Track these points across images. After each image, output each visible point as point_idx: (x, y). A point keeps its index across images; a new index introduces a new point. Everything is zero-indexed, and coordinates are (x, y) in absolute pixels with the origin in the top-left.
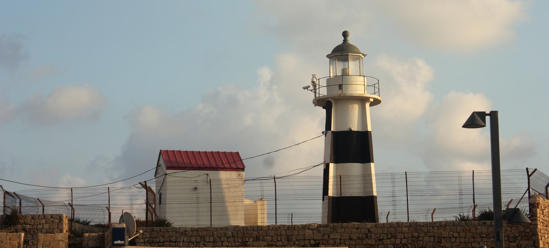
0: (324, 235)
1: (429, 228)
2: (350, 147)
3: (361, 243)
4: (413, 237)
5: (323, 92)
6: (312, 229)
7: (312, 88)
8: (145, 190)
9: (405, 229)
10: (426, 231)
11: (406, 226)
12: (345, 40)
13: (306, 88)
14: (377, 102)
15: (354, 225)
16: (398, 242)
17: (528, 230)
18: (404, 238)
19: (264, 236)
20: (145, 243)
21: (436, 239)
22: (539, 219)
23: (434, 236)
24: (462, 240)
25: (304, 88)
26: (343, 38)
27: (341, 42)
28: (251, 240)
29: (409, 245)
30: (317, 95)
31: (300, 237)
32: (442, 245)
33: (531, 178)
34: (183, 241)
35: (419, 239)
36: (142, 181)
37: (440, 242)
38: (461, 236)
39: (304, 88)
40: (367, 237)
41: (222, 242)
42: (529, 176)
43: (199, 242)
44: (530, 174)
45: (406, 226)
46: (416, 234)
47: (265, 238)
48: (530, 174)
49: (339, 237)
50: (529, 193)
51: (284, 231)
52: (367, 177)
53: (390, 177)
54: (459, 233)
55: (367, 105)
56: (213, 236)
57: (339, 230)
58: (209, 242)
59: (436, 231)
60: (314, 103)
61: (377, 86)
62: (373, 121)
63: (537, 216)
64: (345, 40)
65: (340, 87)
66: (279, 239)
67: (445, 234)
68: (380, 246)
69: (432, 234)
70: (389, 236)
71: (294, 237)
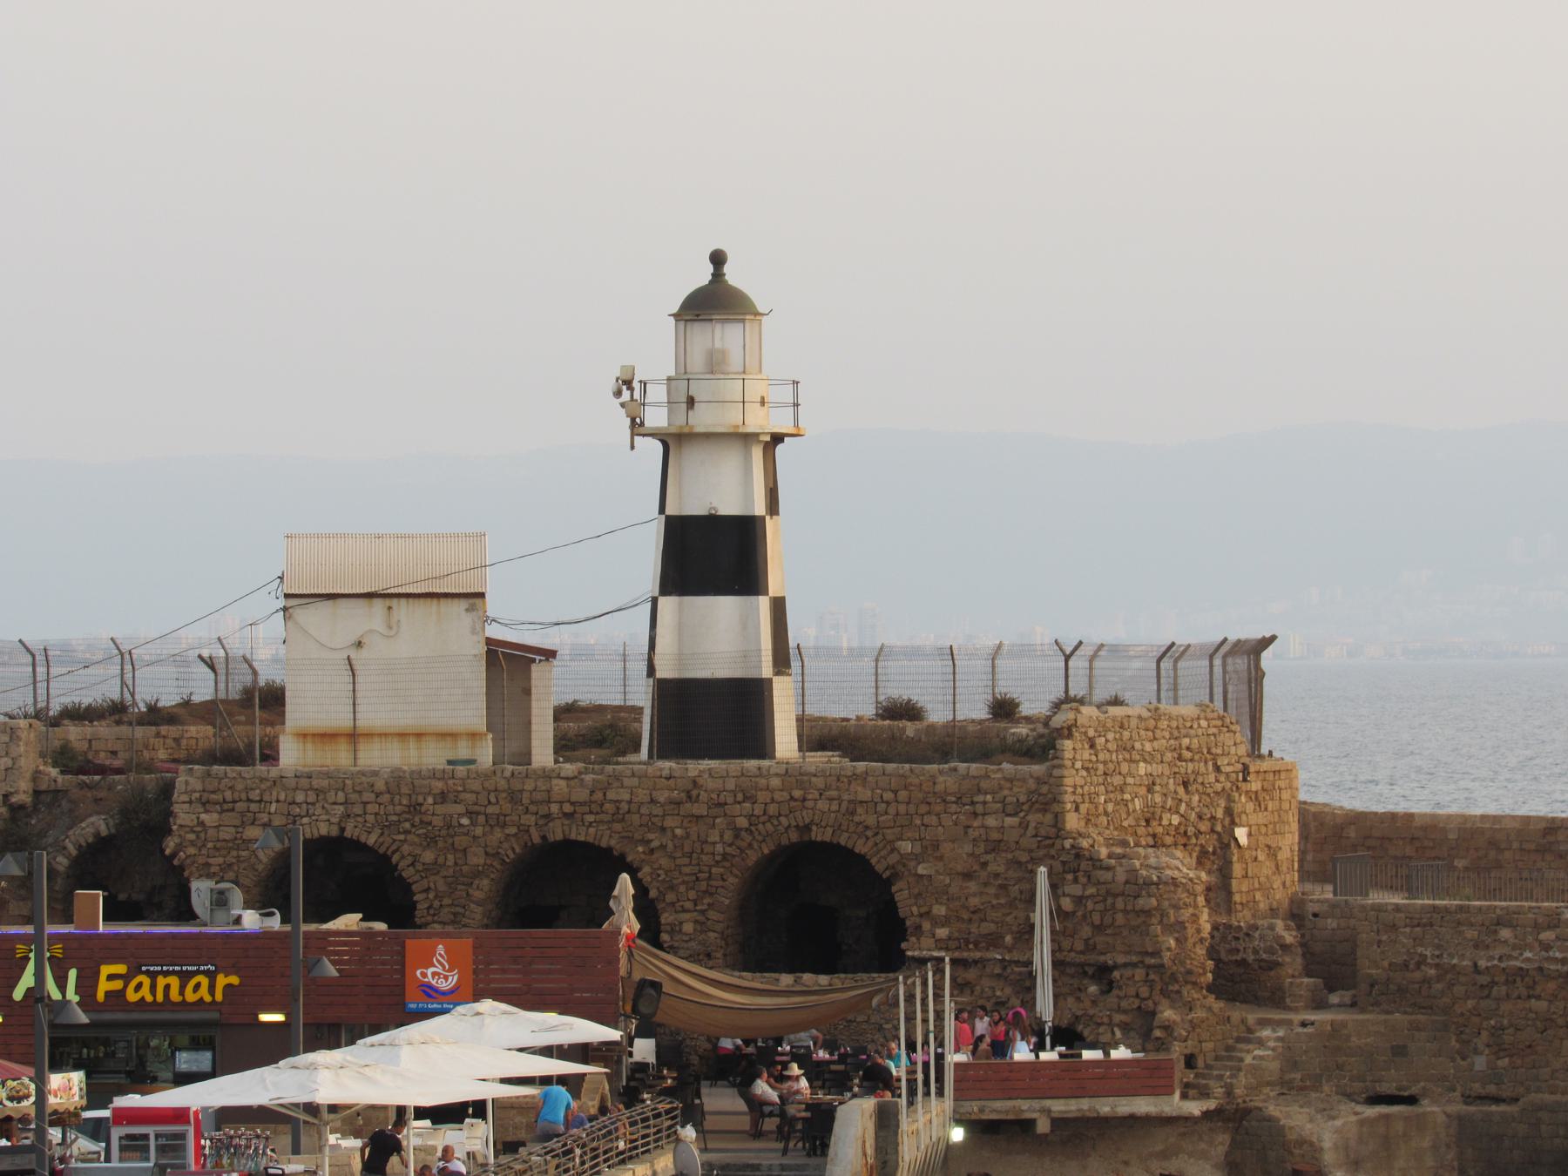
0: (592, 792)
4: (792, 798)
6: (567, 778)
11: (777, 775)
20: (190, 802)
21: (844, 805)
23: (839, 798)
24: (902, 808)
28: (430, 800)
31: (538, 796)
37: (853, 813)
38: (900, 799)
40: (690, 797)
41: (365, 803)
46: (797, 793)
47: (462, 796)
49: (627, 797)
54: (895, 792)
57: (627, 782)
69: (834, 793)
70: (740, 797)
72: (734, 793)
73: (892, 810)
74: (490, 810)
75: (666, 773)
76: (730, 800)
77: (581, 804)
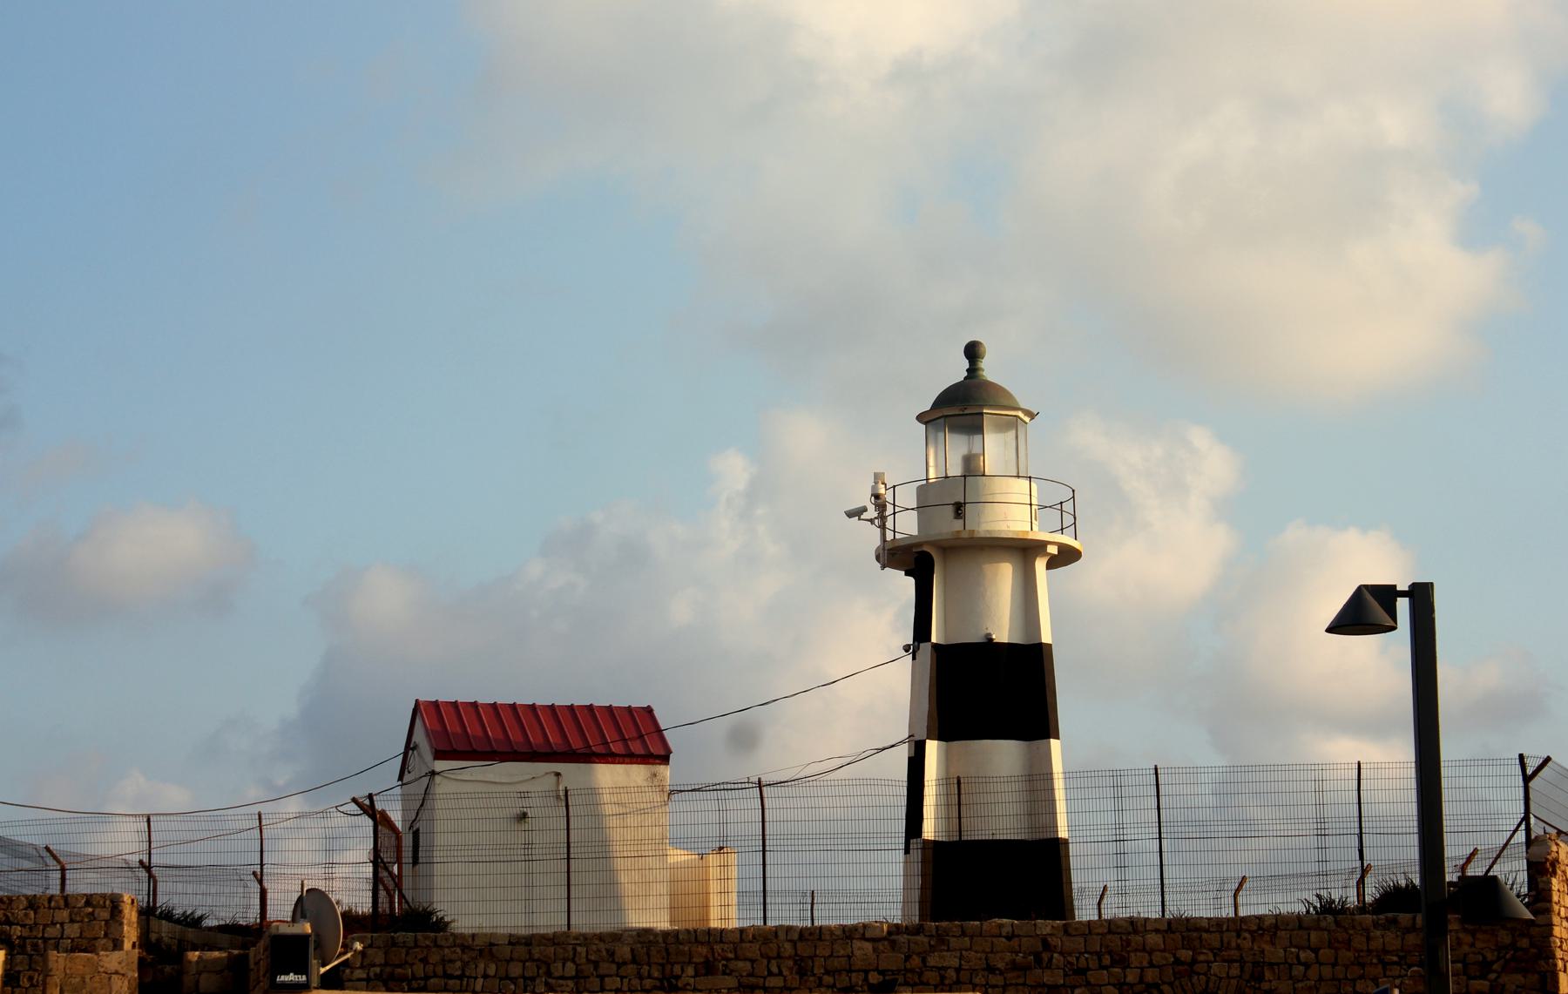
0: (908, 958)
1: (1226, 937)
2: (989, 690)
3: (1021, 981)
4: (1177, 961)
5: (907, 525)
6: (873, 940)
7: (872, 513)
8: (371, 822)
9: (1154, 939)
10: (1217, 944)
11: (1157, 931)
12: (973, 371)
13: (857, 513)
14: (1067, 556)
15: (1001, 926)
16: (1131, 977)
17: (1524, 943)
18: (1151, 965)
19: (728, 959)
20: (368, 980)
22: (1556, 908)
23: (1241, 961)
24: (1327, 971)
25: (850, 514)
26: (966, 364)
28: (690, 971)
29: (1165, 988)
30: (889, 536)
31: (836, 963)
33: (1531, 784)
34: (485, 976)
35: (1198, 967)
36: (361, 793)
37: (1261, 978)
39: (850, 514)
42: (1527, 779)
43: (533, 979)
44: (1529, 771)
45: (1157, 931)
46: (1186, 954)
47: (732, 965)
48: (1529, 771)
49: (955, 962)
50: (1528, 830)
51: (788, 946)
52: (1038, 783)
53: (1109, 782)
54: (1316, 951)
55: (1040, 564)
56: (573, 961)
57: (953, 942)
58: (562, 978)
59: (1247, 944)
60: (878, 558)
61: (1068, 507)
62: (1060, 612)
63: (1550, 901)
64: (973, 371)
65: (959, 509)
66: (775, 970)
67: (1275, 953)
68: (1077, 991)
69: (1235, 954)
70: (1107, 960)
71: (819, 962)
72: (1099, 955)
73: (1313, 973)
75: (1006, 930)
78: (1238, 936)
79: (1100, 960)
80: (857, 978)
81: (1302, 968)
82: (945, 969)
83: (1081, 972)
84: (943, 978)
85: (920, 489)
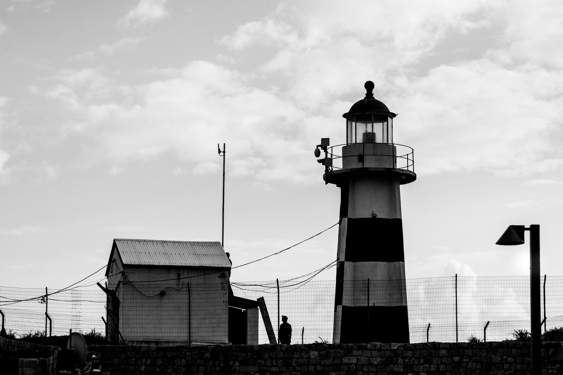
0: (334, 360)
2: (373, 241)
3: (384, 370)
4: (454, 362)
5: (338, 165)
10: (470, 354)
15: (375, 346)
18: (442, 363)
27: (362, 97)
28: (237, 364)
29: (447, 373)
32: (492, 373)
34: (146, 364)
38: (518, 361)
49: (355, 361)
54: (514, 357)
56: (185, 359)
60: (324, 179)
61: (410, 157)
67: (497, 359)
70: (422, 361)
74: (273, 369)
76: (416, 363)
77: (327, 366)
78: (481, 351)
79: (419, 361)
80: (311, 368)
81: (508, 365)
82: (351, 364)
83: (412, 366)
84: (349, 368)
85: (343, 148)
